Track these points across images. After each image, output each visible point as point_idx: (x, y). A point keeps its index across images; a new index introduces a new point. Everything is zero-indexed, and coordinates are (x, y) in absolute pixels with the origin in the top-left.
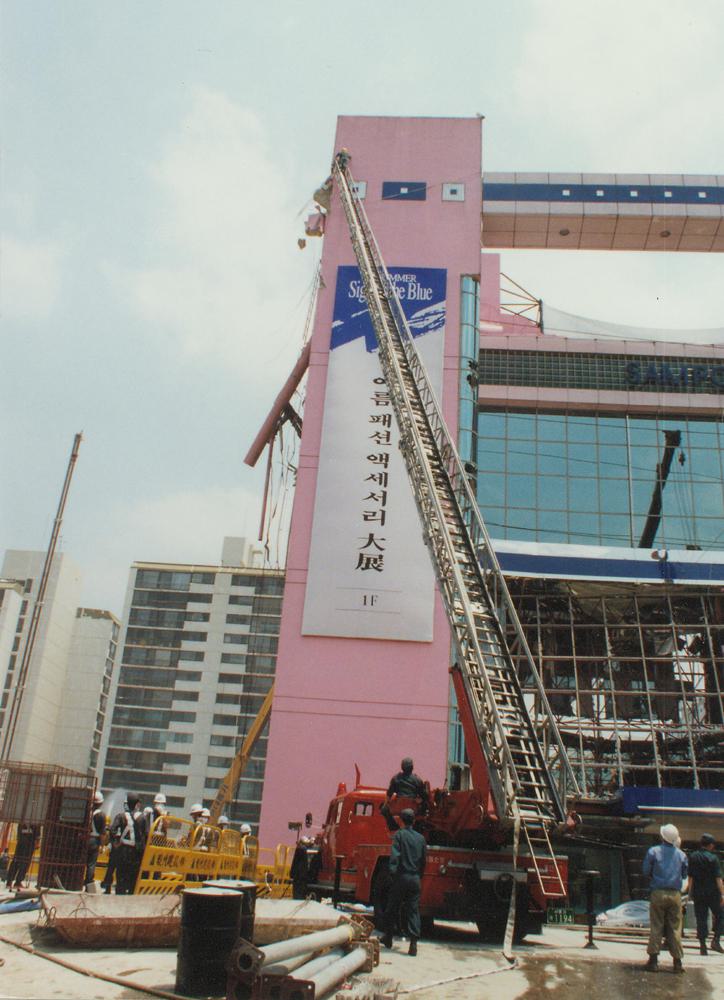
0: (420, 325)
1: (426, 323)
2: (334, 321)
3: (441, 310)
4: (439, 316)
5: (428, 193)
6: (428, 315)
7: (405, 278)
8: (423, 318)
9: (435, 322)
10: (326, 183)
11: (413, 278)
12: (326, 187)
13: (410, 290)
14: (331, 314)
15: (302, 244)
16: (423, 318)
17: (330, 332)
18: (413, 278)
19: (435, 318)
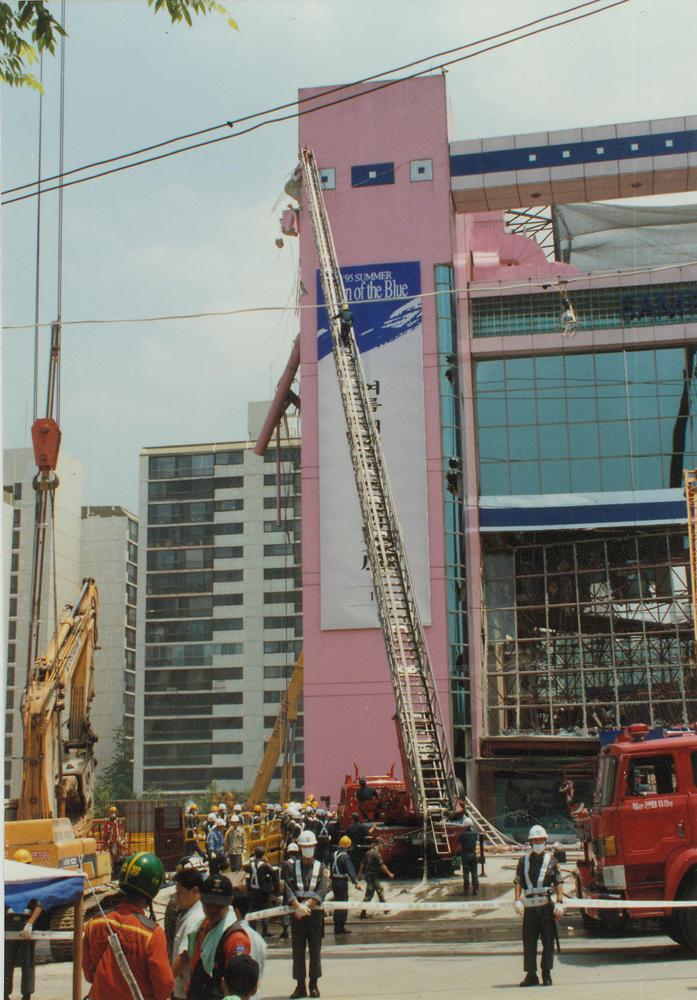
0: (398, 325)
1: (404, 321)
2: (318, 329)
3: (417, 307)
4: (416, 312)
5: (397, 175)
6: (405, 312)
7: (381, 276)
8: (401, 316)
9: (412, 320)
10: (296, 173)
11: (389, 274)
12: (296, 179)
13: (387, 289)
14: (316, 327)
15: (280, 243)
16: (401, 316)
17: (316, 343)
18: (389, 274)
19: (410, 316)
